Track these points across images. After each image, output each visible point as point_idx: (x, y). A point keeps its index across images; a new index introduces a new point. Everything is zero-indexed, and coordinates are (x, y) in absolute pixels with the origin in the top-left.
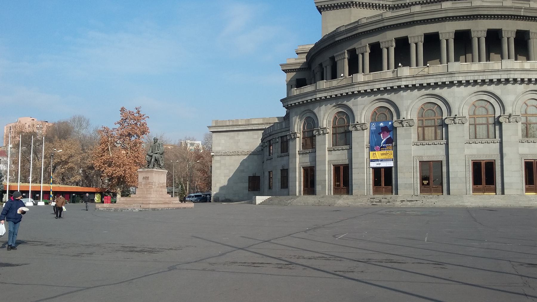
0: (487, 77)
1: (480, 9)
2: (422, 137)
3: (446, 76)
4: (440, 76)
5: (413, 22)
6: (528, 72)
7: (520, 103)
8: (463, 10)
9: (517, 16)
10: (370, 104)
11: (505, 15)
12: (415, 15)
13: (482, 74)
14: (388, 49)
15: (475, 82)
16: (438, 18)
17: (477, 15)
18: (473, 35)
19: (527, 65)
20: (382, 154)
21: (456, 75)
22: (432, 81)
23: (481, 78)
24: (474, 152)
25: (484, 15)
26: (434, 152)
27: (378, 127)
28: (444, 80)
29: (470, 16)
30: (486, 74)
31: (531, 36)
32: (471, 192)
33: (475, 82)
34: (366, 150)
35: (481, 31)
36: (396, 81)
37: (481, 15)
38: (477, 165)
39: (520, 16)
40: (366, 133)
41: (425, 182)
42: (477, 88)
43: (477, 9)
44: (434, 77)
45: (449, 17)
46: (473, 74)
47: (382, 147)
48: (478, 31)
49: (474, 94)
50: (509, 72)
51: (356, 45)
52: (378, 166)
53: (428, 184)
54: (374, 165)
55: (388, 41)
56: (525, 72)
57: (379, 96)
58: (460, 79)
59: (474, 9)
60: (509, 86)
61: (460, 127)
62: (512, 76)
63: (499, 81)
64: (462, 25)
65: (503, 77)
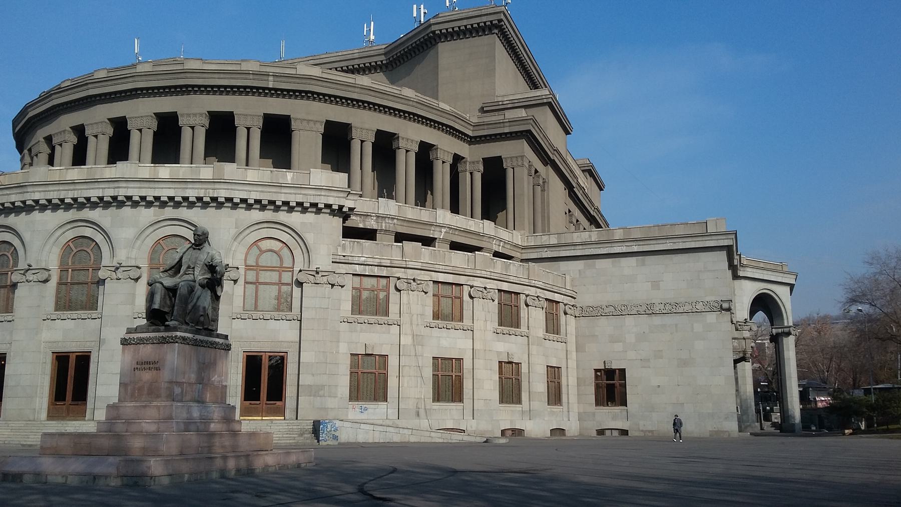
0: (81, 193)
1: (188, 75)
3: (15, 191)
4: (8, 192)
6: (152, 185)
7: (150, 242)
9: (264, 89)
11: (239, 87)
12: (90, 86)
13: (72, 187)
16: (125, 91)
17: (187, 86)
18: (182, 122)
19: (289, 176)
21: (30, 189)
23: (71, 194)
25: (199, 86)
28: (13, 198)
30: (78, 187)
31: (294, 125)
32: (44, 415)
35: (195, 115)
37: (193, 86)
38: (61, 360)
39: (270, 89)
42: (72, 214)
45: (142, 89)
48: (189, 115)
49: (69, 226)
50: (116, 185)
51: (33, 142)
55: (60, 133)
56: (146, 185)
58: (37, 196)
60: (127, 210)
61: (38, 287)
62: (122, 193)
63: (102, 203)
64: (166, 104)
65: (108, 193)
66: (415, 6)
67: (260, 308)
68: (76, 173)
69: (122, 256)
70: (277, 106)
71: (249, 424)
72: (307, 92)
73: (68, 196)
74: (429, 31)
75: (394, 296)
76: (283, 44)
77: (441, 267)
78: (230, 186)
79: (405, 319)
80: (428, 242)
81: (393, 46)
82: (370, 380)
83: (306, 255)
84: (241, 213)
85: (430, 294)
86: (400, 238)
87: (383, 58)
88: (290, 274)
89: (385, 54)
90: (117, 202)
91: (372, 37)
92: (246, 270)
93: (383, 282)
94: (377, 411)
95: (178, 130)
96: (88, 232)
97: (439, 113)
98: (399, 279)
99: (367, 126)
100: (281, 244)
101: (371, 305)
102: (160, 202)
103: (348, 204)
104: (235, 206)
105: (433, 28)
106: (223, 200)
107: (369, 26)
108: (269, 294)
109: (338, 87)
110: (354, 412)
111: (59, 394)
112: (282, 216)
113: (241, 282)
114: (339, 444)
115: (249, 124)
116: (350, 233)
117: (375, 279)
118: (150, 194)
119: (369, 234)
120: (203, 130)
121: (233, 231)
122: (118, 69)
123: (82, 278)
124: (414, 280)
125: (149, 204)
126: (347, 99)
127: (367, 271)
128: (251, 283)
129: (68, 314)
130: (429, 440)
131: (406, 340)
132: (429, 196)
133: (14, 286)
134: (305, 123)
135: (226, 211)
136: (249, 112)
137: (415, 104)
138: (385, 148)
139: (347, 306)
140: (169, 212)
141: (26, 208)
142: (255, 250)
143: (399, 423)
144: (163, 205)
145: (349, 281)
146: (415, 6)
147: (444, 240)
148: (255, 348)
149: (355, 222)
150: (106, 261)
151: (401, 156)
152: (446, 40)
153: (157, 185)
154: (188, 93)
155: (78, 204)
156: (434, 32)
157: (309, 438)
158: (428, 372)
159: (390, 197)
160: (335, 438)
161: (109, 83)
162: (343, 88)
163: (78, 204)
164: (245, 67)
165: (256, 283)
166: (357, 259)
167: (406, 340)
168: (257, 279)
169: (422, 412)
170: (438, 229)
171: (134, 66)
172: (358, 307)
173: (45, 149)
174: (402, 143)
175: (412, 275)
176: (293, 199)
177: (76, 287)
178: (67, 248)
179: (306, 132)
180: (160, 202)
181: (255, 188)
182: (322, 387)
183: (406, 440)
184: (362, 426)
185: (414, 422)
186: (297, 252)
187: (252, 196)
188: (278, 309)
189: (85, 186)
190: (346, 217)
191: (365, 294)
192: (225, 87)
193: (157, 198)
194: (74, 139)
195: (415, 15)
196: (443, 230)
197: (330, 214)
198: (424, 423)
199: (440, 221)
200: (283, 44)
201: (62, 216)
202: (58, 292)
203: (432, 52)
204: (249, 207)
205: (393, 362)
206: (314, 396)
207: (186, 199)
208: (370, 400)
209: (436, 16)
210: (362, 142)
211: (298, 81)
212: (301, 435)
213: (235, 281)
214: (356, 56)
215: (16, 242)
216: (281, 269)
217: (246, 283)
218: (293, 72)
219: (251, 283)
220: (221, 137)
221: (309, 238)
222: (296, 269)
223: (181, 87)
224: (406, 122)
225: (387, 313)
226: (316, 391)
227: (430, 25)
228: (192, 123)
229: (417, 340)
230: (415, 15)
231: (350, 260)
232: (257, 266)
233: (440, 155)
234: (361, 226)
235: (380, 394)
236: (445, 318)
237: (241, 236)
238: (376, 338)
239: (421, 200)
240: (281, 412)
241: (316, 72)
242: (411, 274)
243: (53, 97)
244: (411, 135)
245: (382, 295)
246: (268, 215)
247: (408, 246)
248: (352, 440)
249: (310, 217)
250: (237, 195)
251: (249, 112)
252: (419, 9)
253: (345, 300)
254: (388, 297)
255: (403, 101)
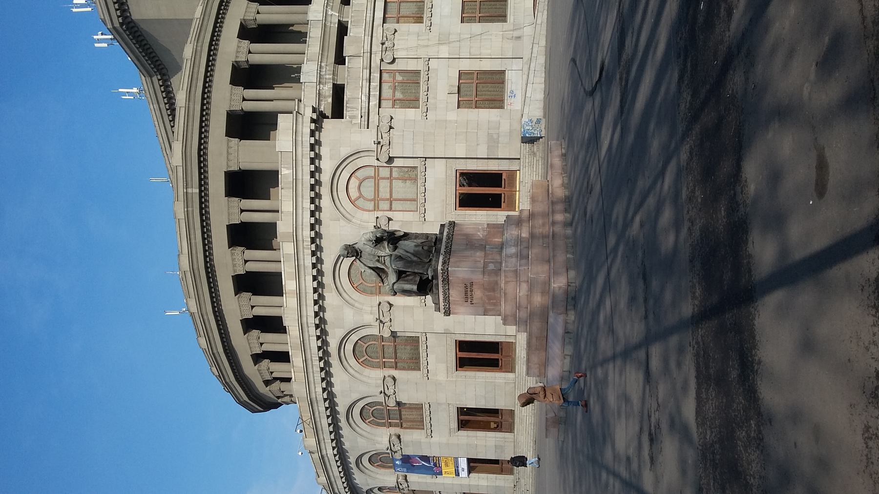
0: (314, 353)
1: (195, 267)
2: (418, 424)
3: (315, 408)
5: (225, 350)
6: (303, 295)
7: (356, 295)
8: (200, 292)
9: (201, 197)
10: (367, 471)
12: (215, 351)
13: (309, 362)
14: (272, 373)
15: (326, 370)
17: (206, 268)
19: (285, 173)
20: (447, 465)
21: (313, 396)
22: (324, 422)
24: (442, 367)
26: (445, 418)
27: (401, 466)
28: (322, 409)
29: (208, 278)
30: (309, 357)
31: (234, 168)
32: (511, 375)
33: (326, 370)
34: (439, 479)
35: (233, 260)
36: (326, 458)
37: (206, 262)
39: (201, 191)
40: (413, 478)
41: (493, 425)
42: (334, 360)
43: (196, 272)
44: (318, 419)
46: (311, 375)
47: (435, 465)
48: (234, 265)
49: (345, 363)
50: (305, 326)
51: (271, 395)
52: (466, 470)
53: (495, 423)
54: (464, 474)
56: (303, 299)
57: (353, 465)
59: (197, 275)
60: (328, 316)
62: (312, 321)
63: (322, 336)
64: (226, 287)
65: (313, 332)
66: (96, 45)
67: (414, 197)
68: (297, 359)
69: (369, 318)
70: (217, 185)
71: (523, 202)
72: (199, 156)
73: (317, 365)
74: (120, 29)
75: (399, 65)
76: (154, 180)
77: (368, 15)
78: (300, 227)
79: (422, 53)
80: (343, 30)
81: (141, 68)
82: (483, 89)
83: (362, 154)
84: (324, 216)
85: (396, 26)
86: (340, 59)
87: (155, 79)
88: (381, 169)
89: (151, 77)
90: (321, 324)
91: (135, 90)
92: (378, 210)
93: (385, 76)
94: (514, 81)
95: (249, 274)
96: (349, 347)
97: (206, 18)
98: (382, 60)
99: (228, 94)
100: (353, 178)
101: (409, 88)
102: (319, 288)
103: (309, 114)
104: (318, 222)
105: (117, 25)
106: (313, 233)
107: (124, 94)
108: (401, 189)
109: (190, 124)
110: (513, 103)
111: (493, 364)
112: (325, 177)
113: (390, 214)
114: (544, 117)
115: (238, 211)
116: (338, 111)
117: (383, 85)
118: (311, 297)
119: (338, 92)
120: (247, 252)
121: (342, 222)
122: (197, 329)
123: (391, 350)
124: (383, 44)
125: (321, 297)
126: (202, 116)
127: (375, 93)
128: (391, 205)
129: (423, 360)
130: (544, 25)
131: (444, 51)
132: (295, 28)
133: (399, 404)
134: (231, 157)
135: (323, 230)
136: (225, 211)
137: (200, 44)
138: (248, 76)
139: (411, 113)
140: (327, 279)
141: (330, 398)
142: (360, 202)
143: (526, 57)
144: (321, 285)
145: (387, 111)
146: (96, 45)
147: (340, 12)
148: (452, 200)
149: (326, 106)
150: (375, 331)
151: (256, 59)
152: (128, 10)
153: (303, 291)
154: (212, 266)
155: (325, 356)
156: (121, 24)
157: (538, 147)
158: (477, 28)
159: (298, 70)
160: (538, 121)
161: (210, 335)
162: (191, 120)
163: (325, 356)
164: (181, 215)
165: (391, 201)
166: (363, 104)
167: (444, 51)
168: (387, 200)
169: (516, 34)
170: (329, 18)
171: (192, 315)
172: (412, 102)
173: (276, 386)
174: (242, 58)
175: (378, 46)
176: (308, 168)
177: (403, 417)
178: (364, 364)
179: (240, 157)
180: (319, 288)
181: (300, 204)
182: (490, 136)
183: (543, 49)
184: (529, 96)
185: (527, 41)
186: (360, 163)
187: (308, 206)
188: (415, 180)
189: (308, 352)
190: (322, 116)
191: (399, 95)
192: (203, 233)
193: (315, 290)
194: (266, 362)
195: (105, 45)
196: (330, 12)
197: (320, 131)
198: (528, 31)
199: (320, 16)
200: (154, 180)
201: (336, 368)
202: (404, 369)
203: (143, 26)
204: (318, 209)
205: (467, 65)
206: (498, 143)
207: (314, 266)
208: (503, 88)
209: (104, 22)
210: (244, 100)
211: (189, 164)
212: (534, 154)
213: (390, 219)
214: (156, 106)
215: (361, 404)
216: (377, 179)
217: (391, 210)
218: (180, 170)
219: (391, 205)
220: (251, 236)
221: (345, 152)
222: (376, 163)
223: (207, 273)
224: (219, 53)
225: (418, 73)
226: (493, 141)
227: (114, 28)
228: (241, 262)
229: (443, 40)
230: (105, 45)
231: (365, 110)
232: (374, 200)
233: (250, 16)
234: (330, 100)
235: (496, 79)
236: (421, 10)
237: (347, 215)
238: (442, 83)
239: (300, 37)
240: (512, 174)
241: (178, 147)
242: (377, 48)
243: (228, 381)
244: (232, 50)
245: (399, 78)
246: (325, 191)
247: (347, 51)
248: (541, 105)
249: (324, 151)
250: (308, 220)
251: (225, 211)
252: (99, 41)
253: (404, 116)
254: (401, 72)
255: (198, 57)
